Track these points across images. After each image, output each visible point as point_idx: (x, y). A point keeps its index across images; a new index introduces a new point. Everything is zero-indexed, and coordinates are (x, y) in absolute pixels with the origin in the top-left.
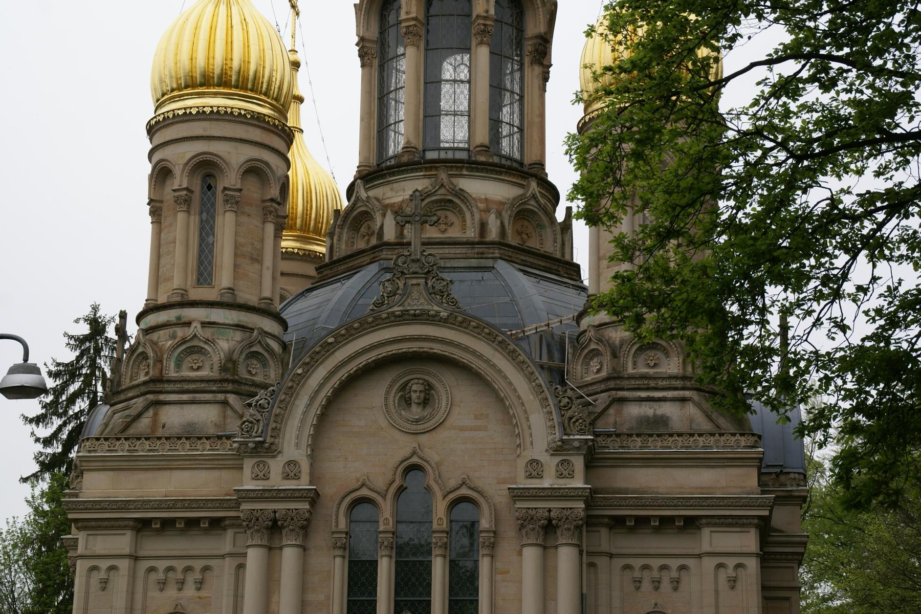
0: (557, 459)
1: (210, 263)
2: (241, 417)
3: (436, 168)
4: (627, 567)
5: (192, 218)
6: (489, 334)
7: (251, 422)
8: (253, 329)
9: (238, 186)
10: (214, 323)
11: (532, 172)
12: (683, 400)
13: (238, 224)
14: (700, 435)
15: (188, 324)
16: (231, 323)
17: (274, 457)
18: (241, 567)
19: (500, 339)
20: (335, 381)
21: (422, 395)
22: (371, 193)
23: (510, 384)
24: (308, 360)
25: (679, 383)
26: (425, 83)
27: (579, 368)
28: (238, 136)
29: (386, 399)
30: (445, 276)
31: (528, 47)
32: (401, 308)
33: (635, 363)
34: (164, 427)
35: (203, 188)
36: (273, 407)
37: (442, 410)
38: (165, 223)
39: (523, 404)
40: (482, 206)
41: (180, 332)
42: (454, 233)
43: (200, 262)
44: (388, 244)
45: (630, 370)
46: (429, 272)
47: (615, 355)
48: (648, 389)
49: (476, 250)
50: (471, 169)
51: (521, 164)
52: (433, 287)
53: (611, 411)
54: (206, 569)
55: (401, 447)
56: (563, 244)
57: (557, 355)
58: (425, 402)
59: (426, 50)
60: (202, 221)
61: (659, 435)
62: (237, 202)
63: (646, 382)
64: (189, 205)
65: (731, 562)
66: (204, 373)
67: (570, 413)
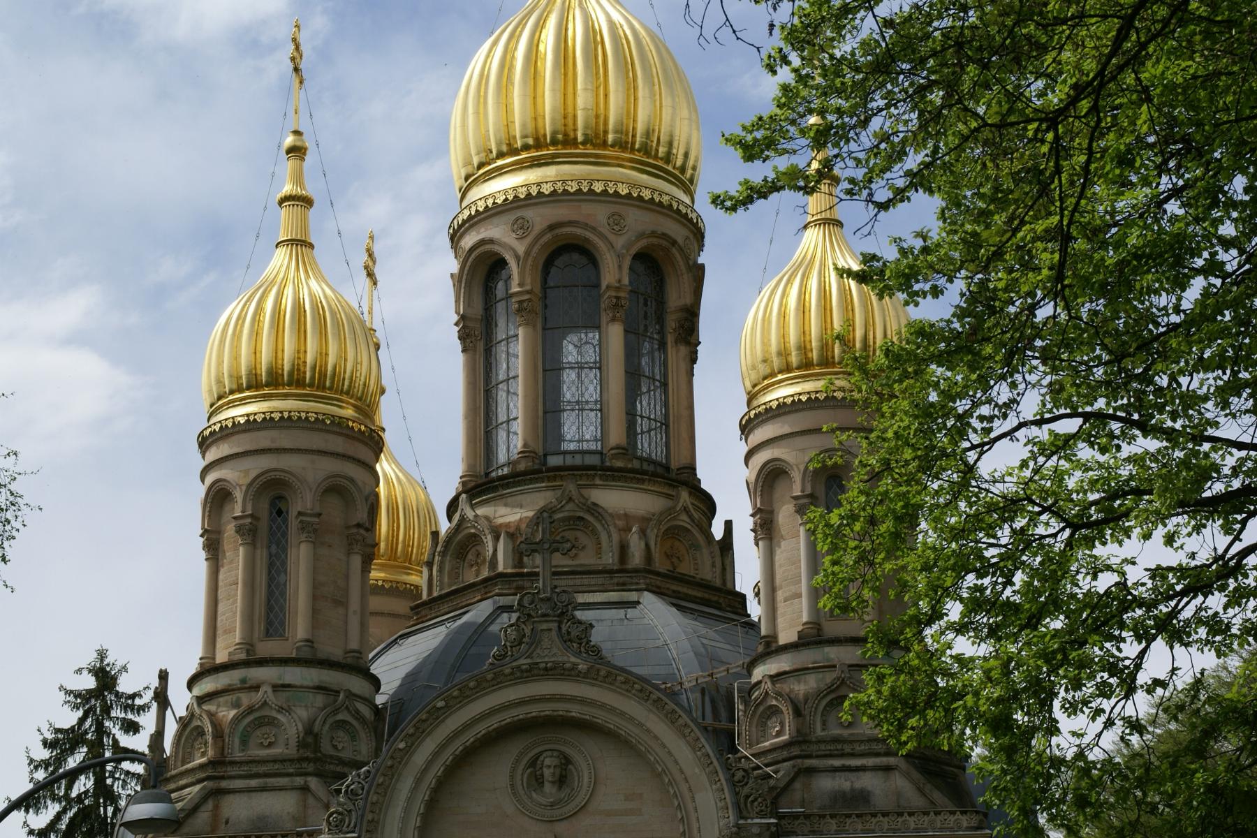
1: (282, 609)
2: (327, 807)
3: (562, 478)
5: (259, 552)
6: (641, 691)
7: (340, 814)
8: (338, 692)
9: (317, 510)
10: (289, 686)
11: (679, 478)
12: (887, 769)
13: (316, 558)
14: (911, 814)
15: (256, 688)
16: (311, 684)
19: (653, 697)
20: (447, 756)
21: (558, 771)
22: (480, 511)
23: (670, 753)
24: (411, 731)
26: (544, 370)
27: (754, 729)
28: (315, 447)
29: (512, 777)
30: (579, 614)
31: (671, 322)
32: (529, 661)
33: (824, 723)
34: (227, 822)
35: (271, 513)
36: (368, 793)
37: (584, 791)
39: (686, 780)
40: (620, 523)
41: (246, 699)
42: (586, 559)
43: (269, 608)
44: (501, 575)
45: (819, 732)
46: (563, 613)
47: (798, 713)
48: (842, 755)
49: (615, 580)
50: (606, 478)
51: (667, 468)
52: (569, 633)
53: (797, 785)
56: (724, 569)
57: (723, 714)
58: (562, 781)
59: (544, 329)
60: (270, 555)
61: (858, 816)
62: (315, 531)
63: (839, 747)
64: (254, 536)
66: (276, 751)
67: (746, 790)
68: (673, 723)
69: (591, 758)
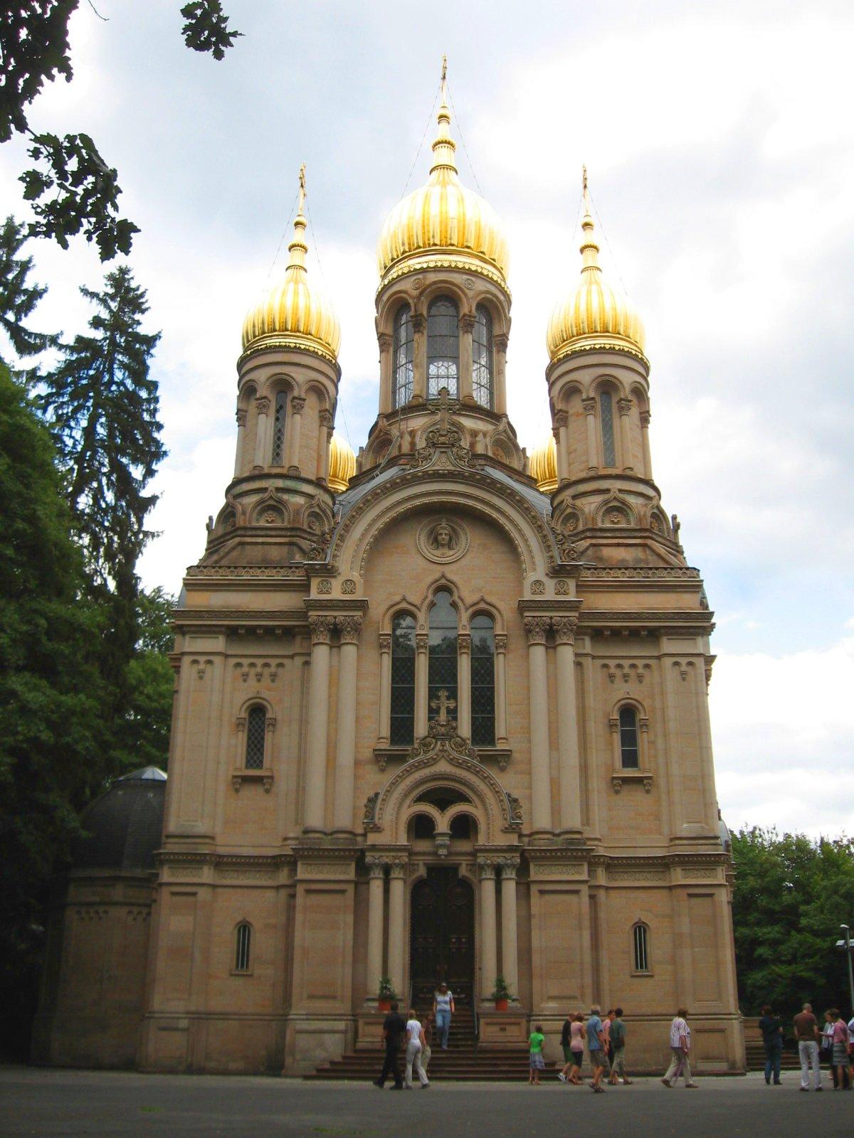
4: (605, 666)
17: (335, 577)
18: (307, 663)
38: (249, 424)
54: (281, 665)
55: (434, 573)
65: (684, 661)
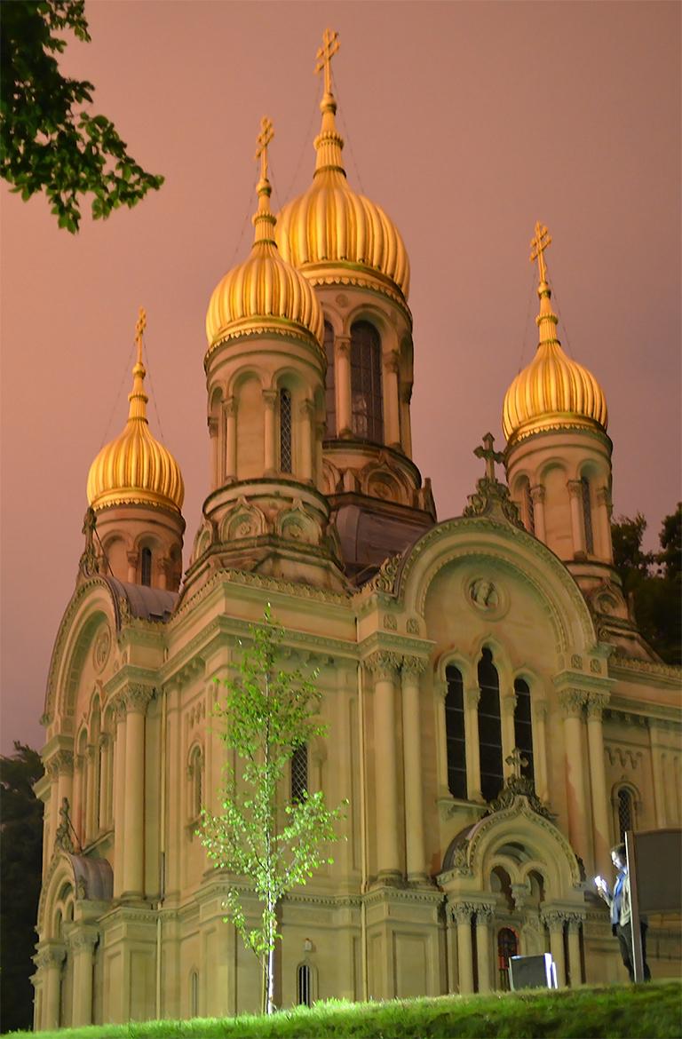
0: (591, 658)
25: (626, 625)
68: (560, 578)
69: (506, 592)
